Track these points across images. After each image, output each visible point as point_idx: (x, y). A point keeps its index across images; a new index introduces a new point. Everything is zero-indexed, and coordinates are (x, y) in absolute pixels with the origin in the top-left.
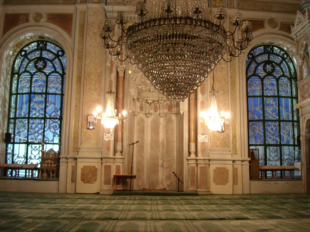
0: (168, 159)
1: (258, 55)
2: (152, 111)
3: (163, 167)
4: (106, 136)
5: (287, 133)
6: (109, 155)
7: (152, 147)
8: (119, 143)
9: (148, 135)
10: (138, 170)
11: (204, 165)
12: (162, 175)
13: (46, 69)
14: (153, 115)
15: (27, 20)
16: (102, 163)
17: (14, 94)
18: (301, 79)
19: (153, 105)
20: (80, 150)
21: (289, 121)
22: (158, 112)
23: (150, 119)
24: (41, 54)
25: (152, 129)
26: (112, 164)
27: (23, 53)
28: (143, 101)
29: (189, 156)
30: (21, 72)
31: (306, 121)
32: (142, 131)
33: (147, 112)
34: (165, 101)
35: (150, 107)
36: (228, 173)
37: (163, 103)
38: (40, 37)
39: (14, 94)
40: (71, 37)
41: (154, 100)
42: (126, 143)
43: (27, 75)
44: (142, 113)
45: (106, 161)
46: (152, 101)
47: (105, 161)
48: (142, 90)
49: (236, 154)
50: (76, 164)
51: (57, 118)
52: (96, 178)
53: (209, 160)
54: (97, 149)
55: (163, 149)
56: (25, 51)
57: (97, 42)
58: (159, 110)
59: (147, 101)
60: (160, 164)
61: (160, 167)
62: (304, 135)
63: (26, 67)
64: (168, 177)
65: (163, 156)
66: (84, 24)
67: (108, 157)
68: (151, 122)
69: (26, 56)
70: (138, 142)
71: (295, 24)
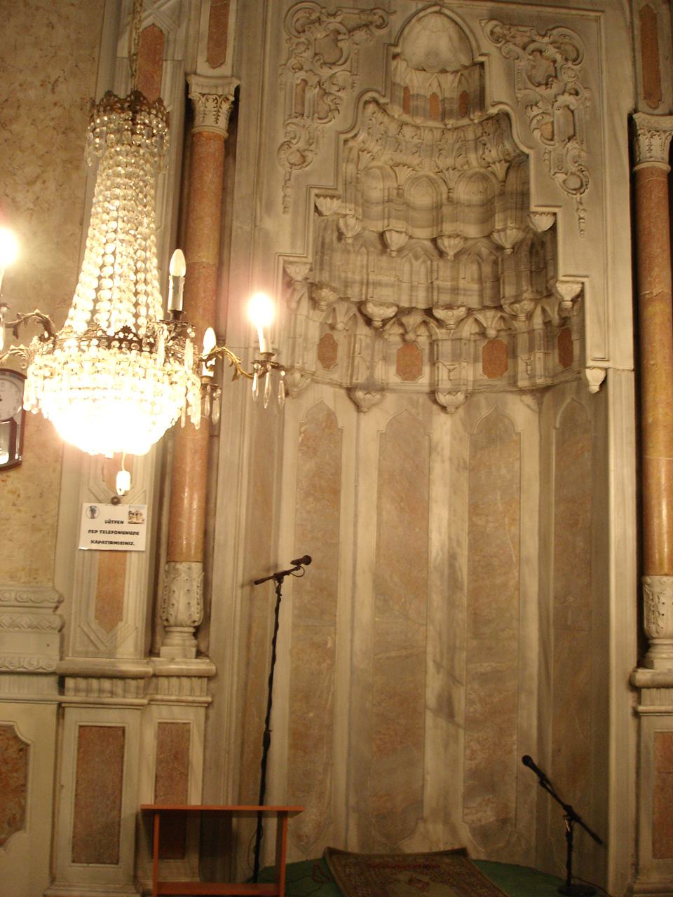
0: (486, 667)
2: (387, 373)
3: (451, 715)
4: (99, 524)
6: (111, 654)
7: (381, 591)
9: (361, 520)
10: (299, 741)
12: (440, 764)
14: (390, 397)
16: (61, 708)
19: (394, 332)
22: (424, 380)
23: (375, 422)
25: (386, 479)
26: (129, 720)
28: (342, 308)
32: (326, 489)
33: (361, 378)
34: (470, 311)
35: (379, 345)
37: (461, 321)
41: (405, 304)
42: (231, 567)
44: (331, 384)
45: (93, 697)
46: (391, 312)
47: (81, 697)
48: (341, 236)
52: (23, 810)
54: (33, 606)
55: (451, 604)
58: (426, 369)
59: (361, 305)
60: (431, 697)
61: (429, 719)
64: (484, 782)
65: (452, 649)
67: (108, 669)
68: (382, 436)
70: (307, 560)
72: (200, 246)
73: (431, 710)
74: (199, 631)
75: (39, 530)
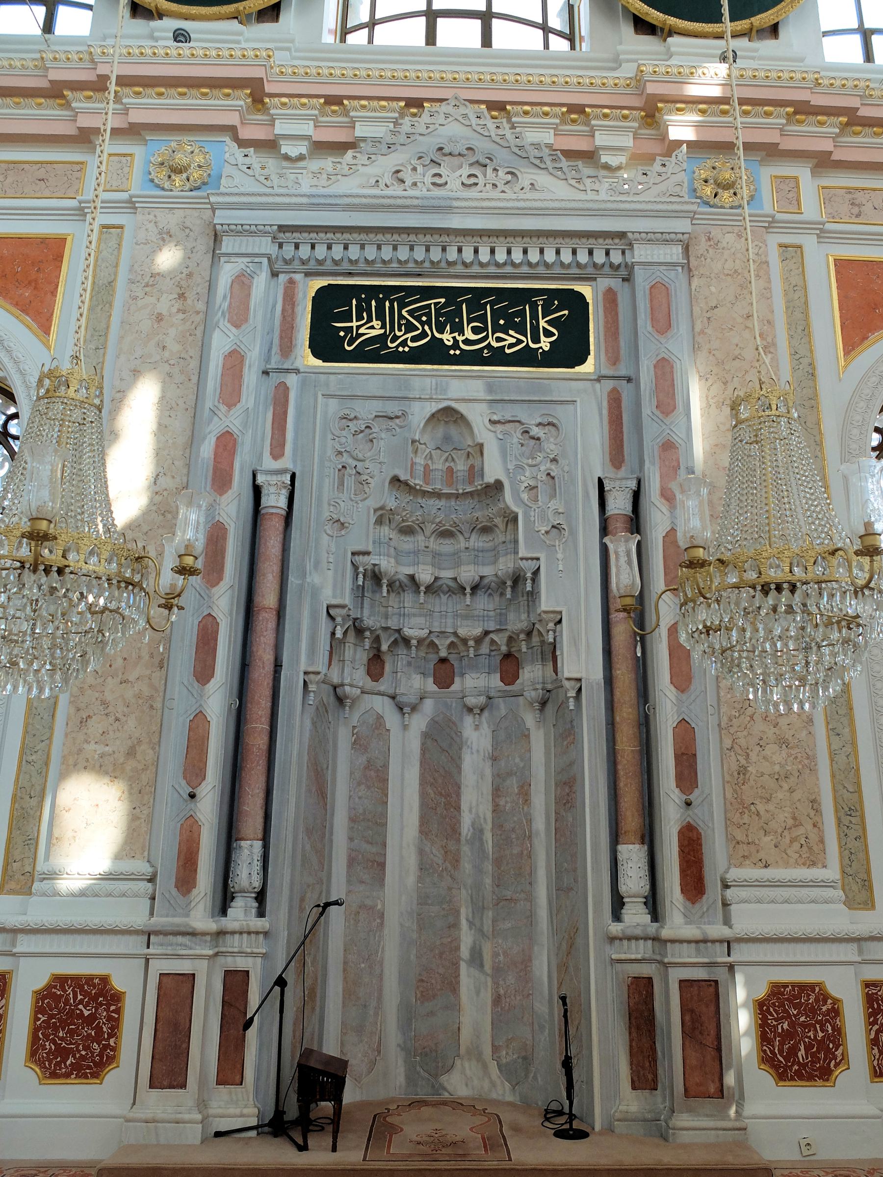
3: (482, 966)
11: (700, 974)
29: (617, 916)
57: (167, 354)
60: (465, 952)
61: (463, 967)
72: (263, 596)
73: (463, 960)
75: (139, 818)
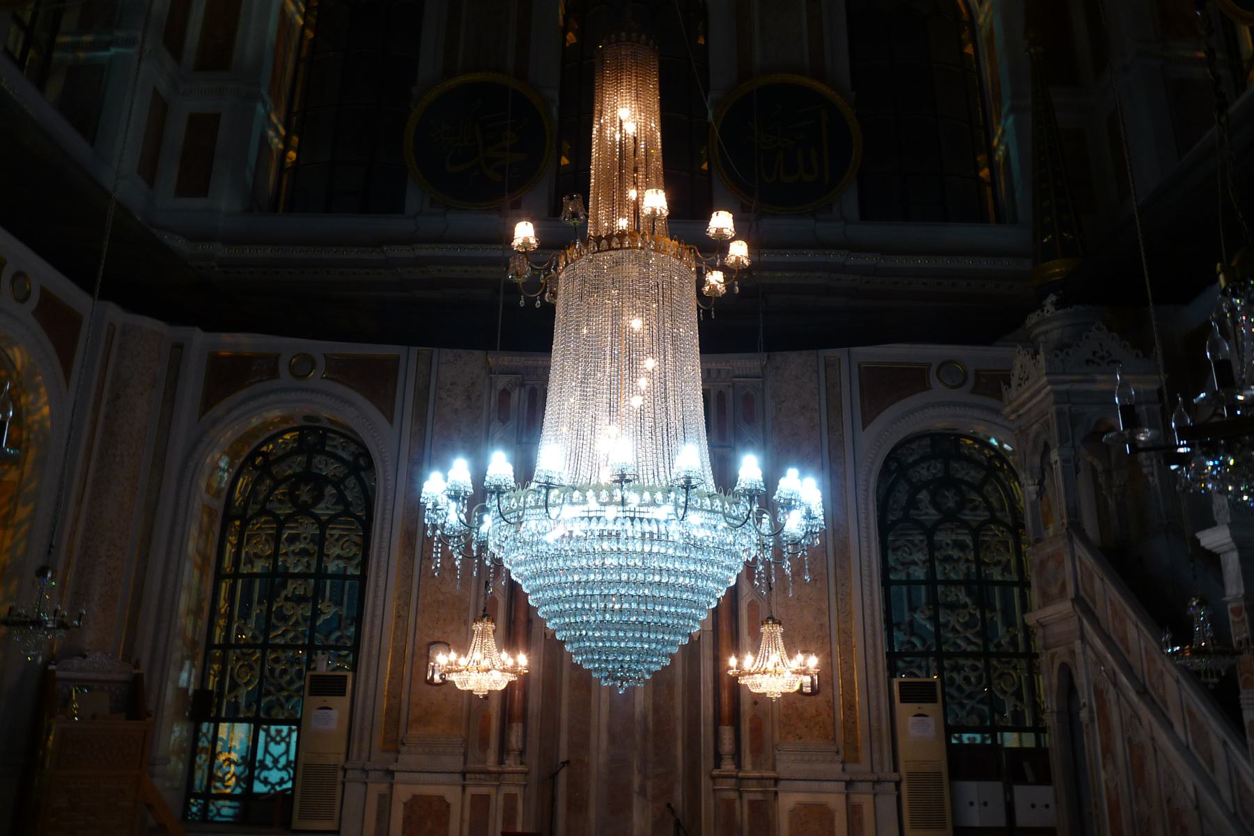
1: (916, 463)
5: (1014, 689)
6: (485, 762)
8: (514, 725)
11: (759, 797)
13: (322, 505)
15: (273, 373)
17: (228, 576)
18: (1038, 540)
20: (404, 749)
21: (1017, 655)
24: (309, 462)
27: (259, 460)
29: (717, 765)
30: (250, 512)
31: (1056, 666)
36: (832, 821)
38: (307, 418)
39: (228, 576)
40: (391, 421)
43: (266, 522)
49: (857, 760)
50: (391, 786)
51: (345, 648)
53: (776, 781)
56: (264, 454)
62: (1055, 708)
63: (267, 499)
66: (427, 387)
69: (265, 470)
71: (1014, 381)
74: (522, 753)
